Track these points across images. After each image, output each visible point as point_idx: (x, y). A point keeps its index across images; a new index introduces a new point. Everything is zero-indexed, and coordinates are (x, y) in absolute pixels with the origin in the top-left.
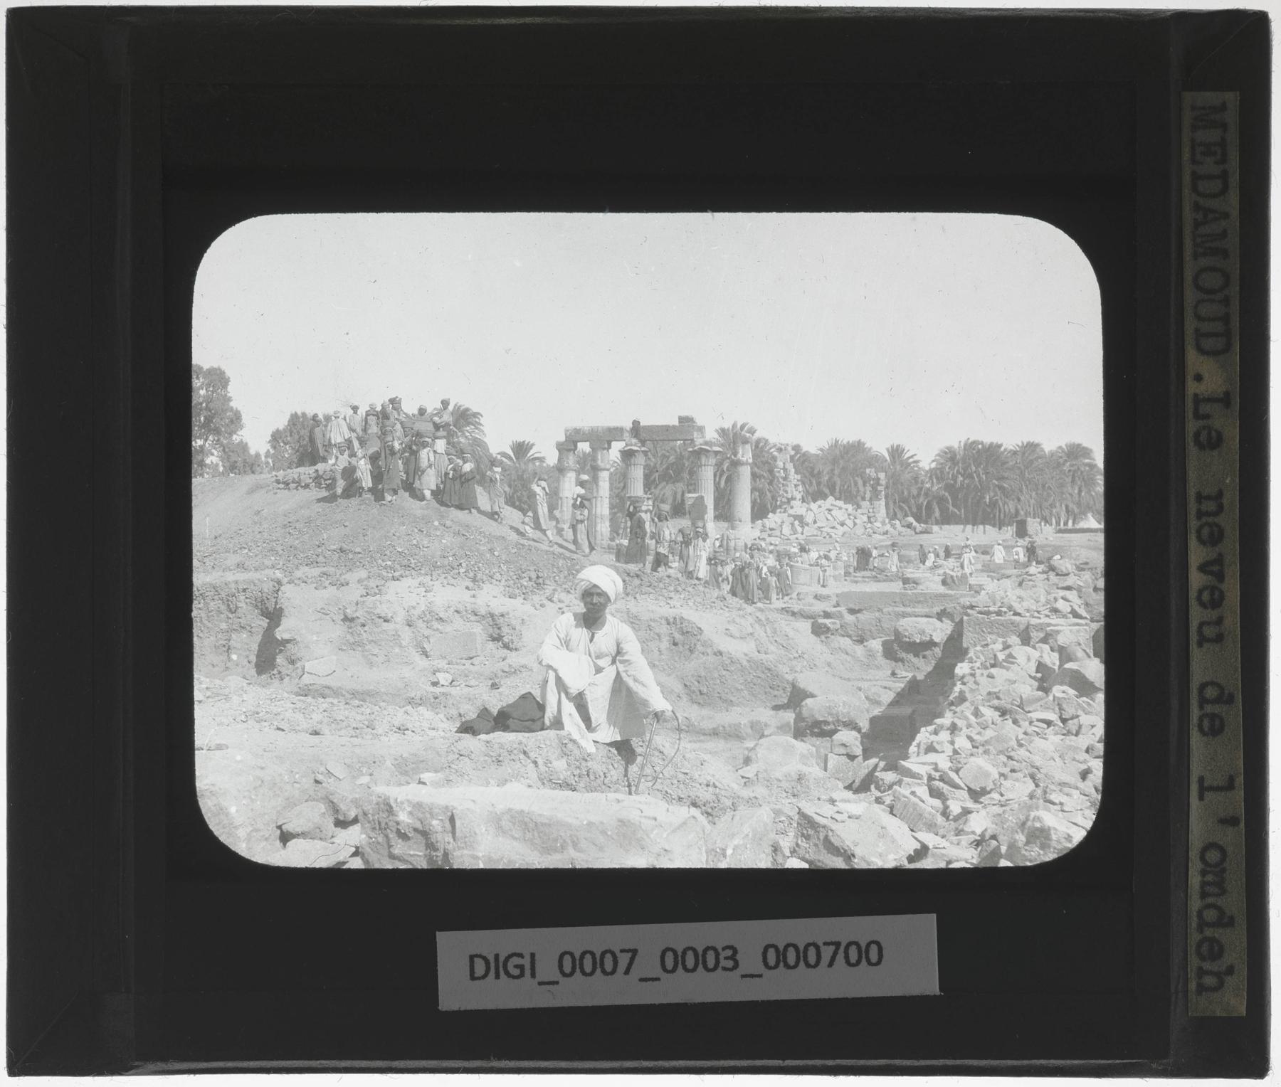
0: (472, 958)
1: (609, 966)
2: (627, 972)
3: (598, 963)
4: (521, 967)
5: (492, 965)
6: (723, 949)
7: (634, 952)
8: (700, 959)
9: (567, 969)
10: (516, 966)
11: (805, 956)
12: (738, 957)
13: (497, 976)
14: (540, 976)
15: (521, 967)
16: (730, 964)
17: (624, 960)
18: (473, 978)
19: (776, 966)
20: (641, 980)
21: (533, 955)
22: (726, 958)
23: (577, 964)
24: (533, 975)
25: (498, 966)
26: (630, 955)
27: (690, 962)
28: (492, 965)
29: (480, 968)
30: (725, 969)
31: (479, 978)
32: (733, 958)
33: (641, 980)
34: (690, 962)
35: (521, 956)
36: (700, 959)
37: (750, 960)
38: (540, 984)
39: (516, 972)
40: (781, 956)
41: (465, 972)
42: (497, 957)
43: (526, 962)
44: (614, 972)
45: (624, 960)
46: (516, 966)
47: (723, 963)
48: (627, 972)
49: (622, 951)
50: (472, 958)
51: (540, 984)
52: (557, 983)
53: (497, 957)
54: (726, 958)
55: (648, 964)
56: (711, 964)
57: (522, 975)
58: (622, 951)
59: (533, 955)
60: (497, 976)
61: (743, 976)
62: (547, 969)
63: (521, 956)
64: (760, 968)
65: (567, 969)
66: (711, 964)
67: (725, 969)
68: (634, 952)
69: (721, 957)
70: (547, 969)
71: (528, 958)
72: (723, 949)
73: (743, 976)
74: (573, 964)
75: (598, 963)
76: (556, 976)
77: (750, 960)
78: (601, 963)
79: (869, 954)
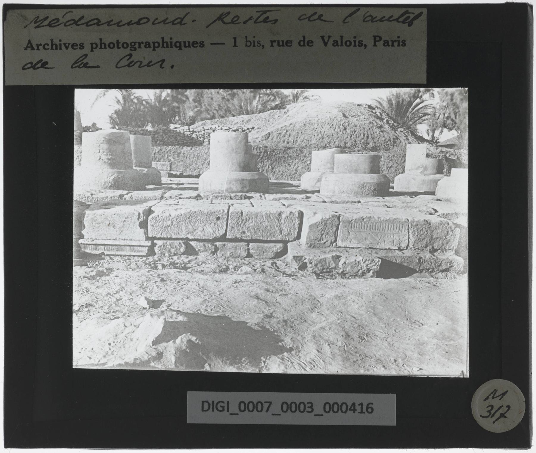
0: (203, 402)
1: (259, 407)
2: (267, 411)
3: (255, 407)
4: (223, 407)
5: (211, 407)
6: (308, 403)
7: (270, 403)
8: (298, 407)
9: (242, 408)
10: (221, 406)
11: (340, 408)
12: (313, 407)
13: (213, 411)
14: (231, 411)
15: (223, 407)
16: (310, 410)
17: (266, 406)
18: (203, 410)
19: (329, 412)
20: (272, 415)
21: (228, 402)
22: (308, 407)
23: (247, 407)
24: (228, 410)
25: (213, 406)
26: (268, 404)
27: (293, 407)
28: (211, 407)
29: (206, 406)
30: (308, 412)
31: (206, 411)
32: (311, 407)
33: (272, 415)
34: (293, 407)
35: (223, 402)
36: (298, 407)
37: (318, 409)
38: (230, 414)
39: (221, 409)
40: (331, 408)
41: (197, 408)
42: (213, 402)
43: (225, 405)
44: (261, 411)
45: (266, 406)
46: (221, 406)
47: (307, 409)
48: (267, 411)
49: (265, 402)
50: (203, 402)
51: (230, 414)
52: (238, 414)
53: (213, 402)
54: (308, 407)
55: (276, 408)
56: (302, 409)
57: (223, 410)
58: (265, 402)
59: (228, 402)
60: (213, 411)
61: (315, 415)
62: (234, 408)
63: (223, 402)
64: (322, 412)
65: (242, 408)
66: (302, 409)
67: (308, 412)
68: (270, 403)
69: (307, 408)
70: (234, 408)
71: (226, 403)
72: (308, 403)
73: (315, 415)
74: (245, 407)
75: (255, 407)
76: (237, 411)
77: (318, 409)
78: (256, 407)
79: (370, 409)
